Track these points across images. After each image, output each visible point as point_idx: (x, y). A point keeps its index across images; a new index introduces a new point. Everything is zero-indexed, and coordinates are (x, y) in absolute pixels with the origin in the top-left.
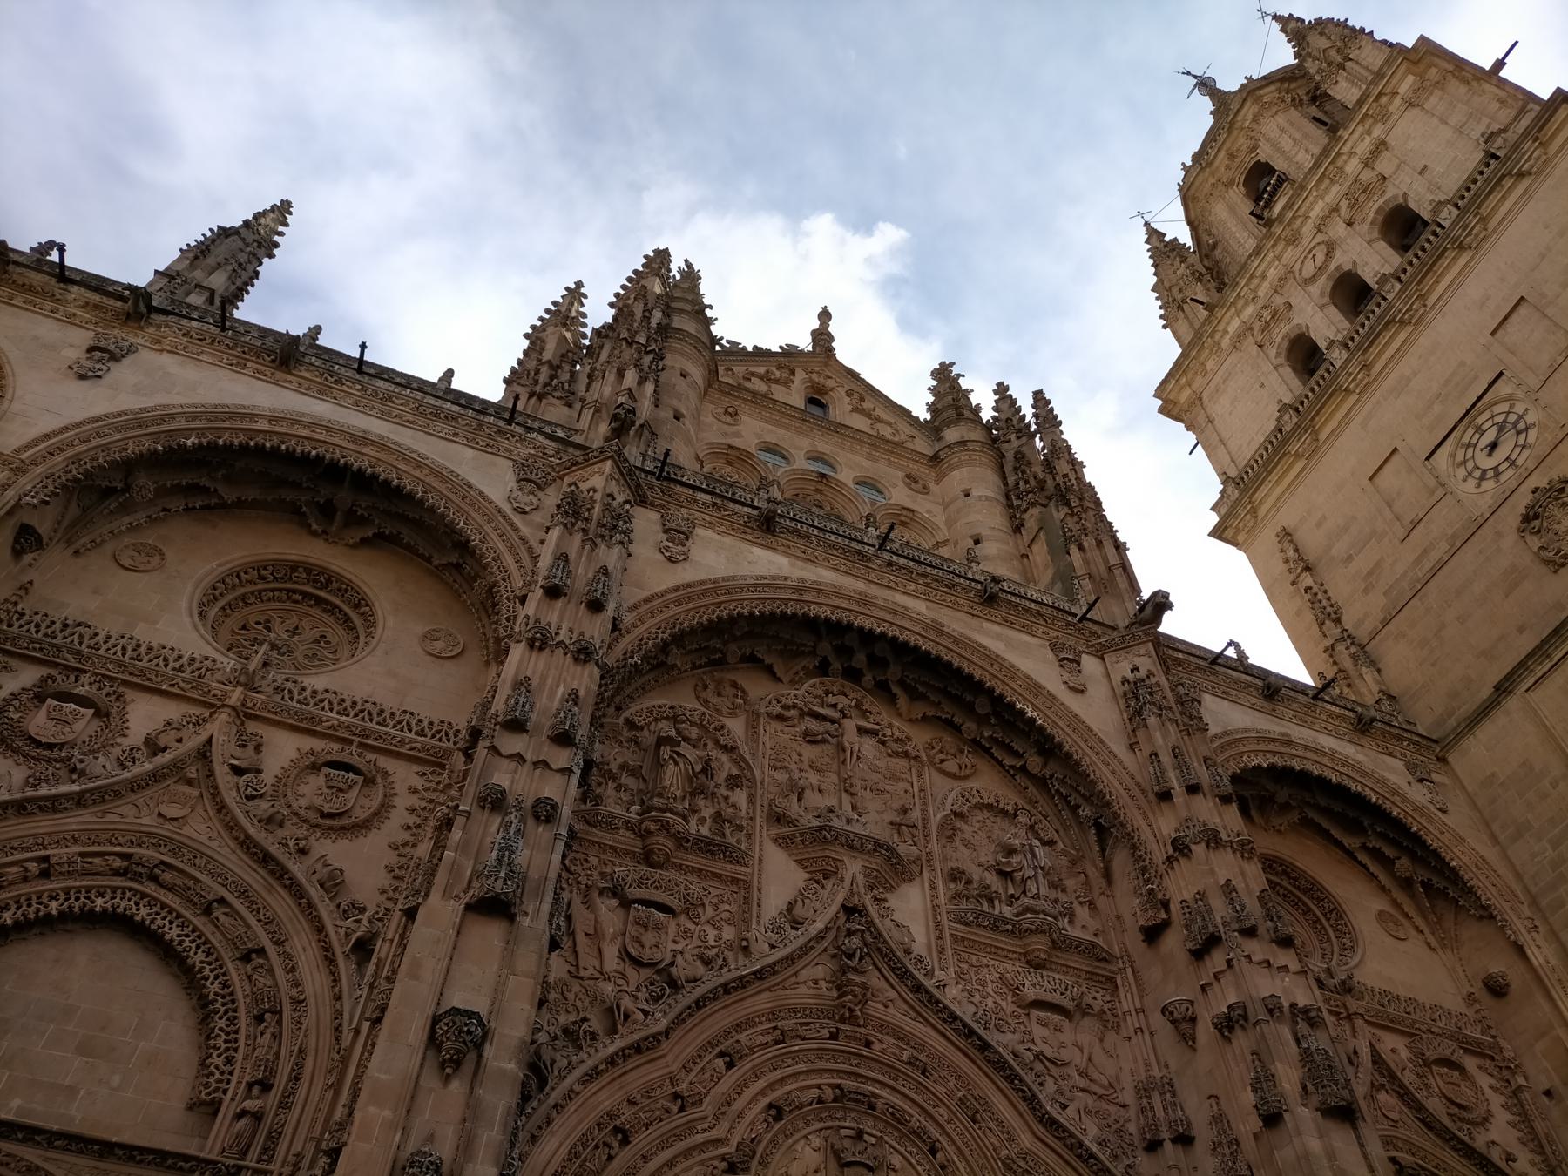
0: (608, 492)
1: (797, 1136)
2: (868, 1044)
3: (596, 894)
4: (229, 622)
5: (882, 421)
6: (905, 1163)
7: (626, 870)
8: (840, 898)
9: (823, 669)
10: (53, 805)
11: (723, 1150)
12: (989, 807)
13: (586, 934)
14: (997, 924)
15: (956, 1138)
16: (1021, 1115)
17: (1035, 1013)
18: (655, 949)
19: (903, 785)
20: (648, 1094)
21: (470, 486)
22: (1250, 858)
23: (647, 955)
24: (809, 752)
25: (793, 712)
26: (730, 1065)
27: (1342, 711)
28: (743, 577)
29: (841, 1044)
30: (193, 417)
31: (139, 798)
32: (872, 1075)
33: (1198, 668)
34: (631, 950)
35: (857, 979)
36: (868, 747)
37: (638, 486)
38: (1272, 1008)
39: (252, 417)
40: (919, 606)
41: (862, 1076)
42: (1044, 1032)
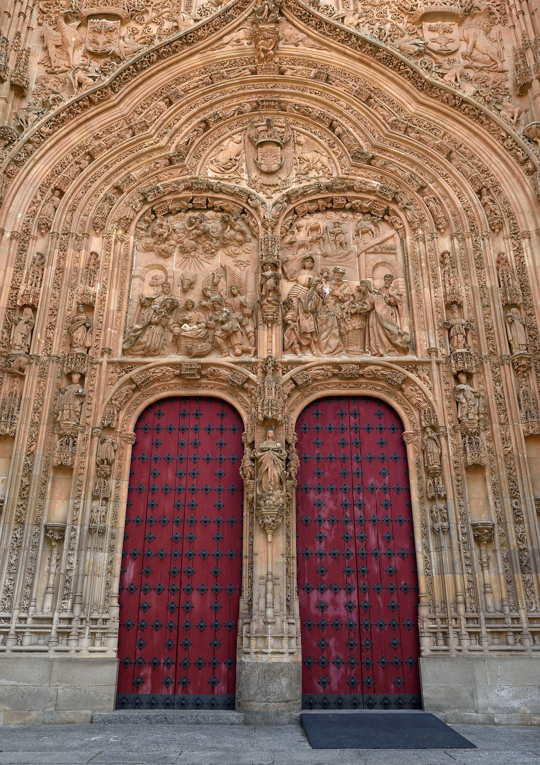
1: (223, 137)
2: (282, 73)
3: (61, 21)
6: (309, 139)
11: (163, 154)
13: (57, 46)
15: (351, 116)
16: (408, 92)
17: (426, 25)
18: (107, 44)
20: (109, 131)
23: (100, 48)
26: (170, 103)
29: (259, 76)
34: (91, 49)
35: (267, 27)
41: (275, 92)
42: (436, 35)
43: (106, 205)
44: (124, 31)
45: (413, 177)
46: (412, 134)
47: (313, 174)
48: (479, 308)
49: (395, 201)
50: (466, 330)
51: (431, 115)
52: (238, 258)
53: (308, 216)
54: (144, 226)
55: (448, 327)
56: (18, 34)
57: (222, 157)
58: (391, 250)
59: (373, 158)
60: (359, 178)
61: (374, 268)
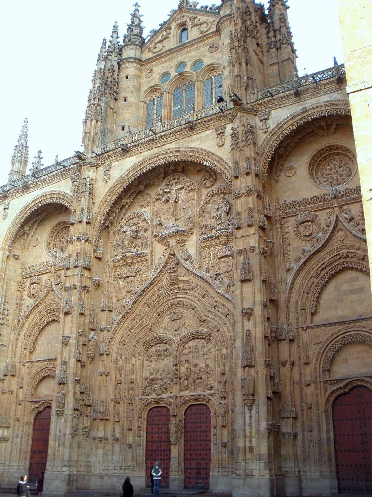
0: (83, 177)
2: (180, 288)
3: (119, 279)
4: (57, 243)
5: (202, 24)
7: (126, 269)
8: (168, 254)
9: (166, 175)
10: (37, 306)
12: (217, 194)
14: (211, 238)
19: (191, 202)
20: (134, 320)
21: (64, 193)
22: (251, 195)
24: (166, 207)
25: (160, 196)
27: (330, 80)
28: (124, 174)
29: (174, 291)
30: (21, 214)
31: (48, 297)
32: (180, 296)
33: (269, 102)
36: (182, 194)
37: (94, 164)
38: (240, 252)
39: (28, 206)
40: (173, 146)
42: (225, 264)
43: (135, 348)
44: (136, 279)
45: (216, 326)
46: (217, 309)
47: (188, 328)
48: (230, 374)
49: (210, 336)
50: (225, 383)
51: (221, 301)
52: (170, 360)
53: (189, 342)
54: (145, 352)
55: (220, 382)
56: (108, 291)
57: (163, 326)
58: (211, 353)
59: (204, 321)
60: (201, 328)
61: (206, 360)
